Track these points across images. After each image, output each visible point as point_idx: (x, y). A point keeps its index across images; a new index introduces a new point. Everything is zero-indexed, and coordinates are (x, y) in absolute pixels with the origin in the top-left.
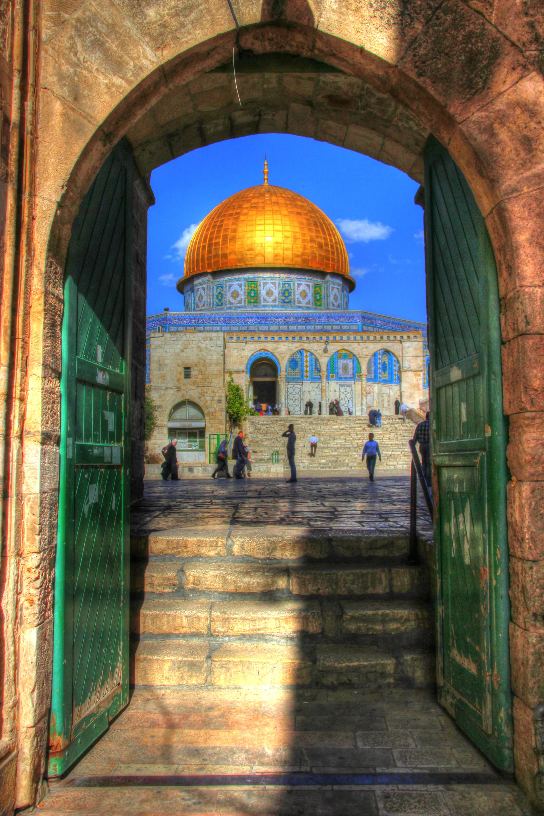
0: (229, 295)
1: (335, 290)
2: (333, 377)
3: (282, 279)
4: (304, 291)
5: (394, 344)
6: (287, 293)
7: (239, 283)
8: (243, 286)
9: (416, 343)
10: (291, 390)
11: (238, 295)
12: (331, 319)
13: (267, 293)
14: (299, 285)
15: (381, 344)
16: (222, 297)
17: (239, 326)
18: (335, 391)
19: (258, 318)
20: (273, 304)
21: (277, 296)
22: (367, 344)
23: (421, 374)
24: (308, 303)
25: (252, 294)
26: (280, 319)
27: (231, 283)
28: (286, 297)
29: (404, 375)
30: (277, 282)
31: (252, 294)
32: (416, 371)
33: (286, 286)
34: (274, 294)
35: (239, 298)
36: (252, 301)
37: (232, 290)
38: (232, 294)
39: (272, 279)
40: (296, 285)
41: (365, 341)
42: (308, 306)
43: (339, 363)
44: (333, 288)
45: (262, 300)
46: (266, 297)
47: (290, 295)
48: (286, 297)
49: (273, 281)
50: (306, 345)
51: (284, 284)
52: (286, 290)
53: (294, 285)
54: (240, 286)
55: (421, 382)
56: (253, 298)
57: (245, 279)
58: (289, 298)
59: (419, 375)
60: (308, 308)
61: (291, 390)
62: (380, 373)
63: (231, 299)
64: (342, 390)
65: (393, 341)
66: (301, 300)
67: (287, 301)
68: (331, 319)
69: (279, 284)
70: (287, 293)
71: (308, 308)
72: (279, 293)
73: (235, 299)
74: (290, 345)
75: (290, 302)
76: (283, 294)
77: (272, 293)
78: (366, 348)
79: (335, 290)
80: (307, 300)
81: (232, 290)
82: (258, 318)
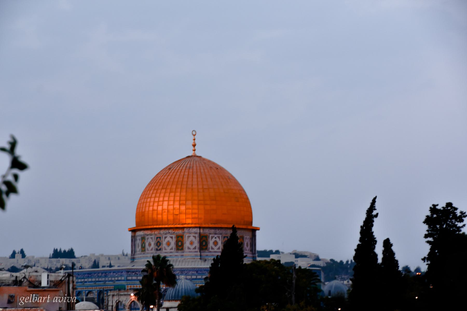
3: (156, 235)
14: (165, 237)
20: (151, 252)
24: (172, 249)
28: (158, 247)
42: (172, 251)
47: (160, 245)
49: (151, 236)
51: (157, 238)
57: (141, 235)
58: (160, 247)
60: (171, 252)
67: (159, 249)
70: (159, 244)
71: (171, 252)
75: (160, 250)
76: (157, 245)
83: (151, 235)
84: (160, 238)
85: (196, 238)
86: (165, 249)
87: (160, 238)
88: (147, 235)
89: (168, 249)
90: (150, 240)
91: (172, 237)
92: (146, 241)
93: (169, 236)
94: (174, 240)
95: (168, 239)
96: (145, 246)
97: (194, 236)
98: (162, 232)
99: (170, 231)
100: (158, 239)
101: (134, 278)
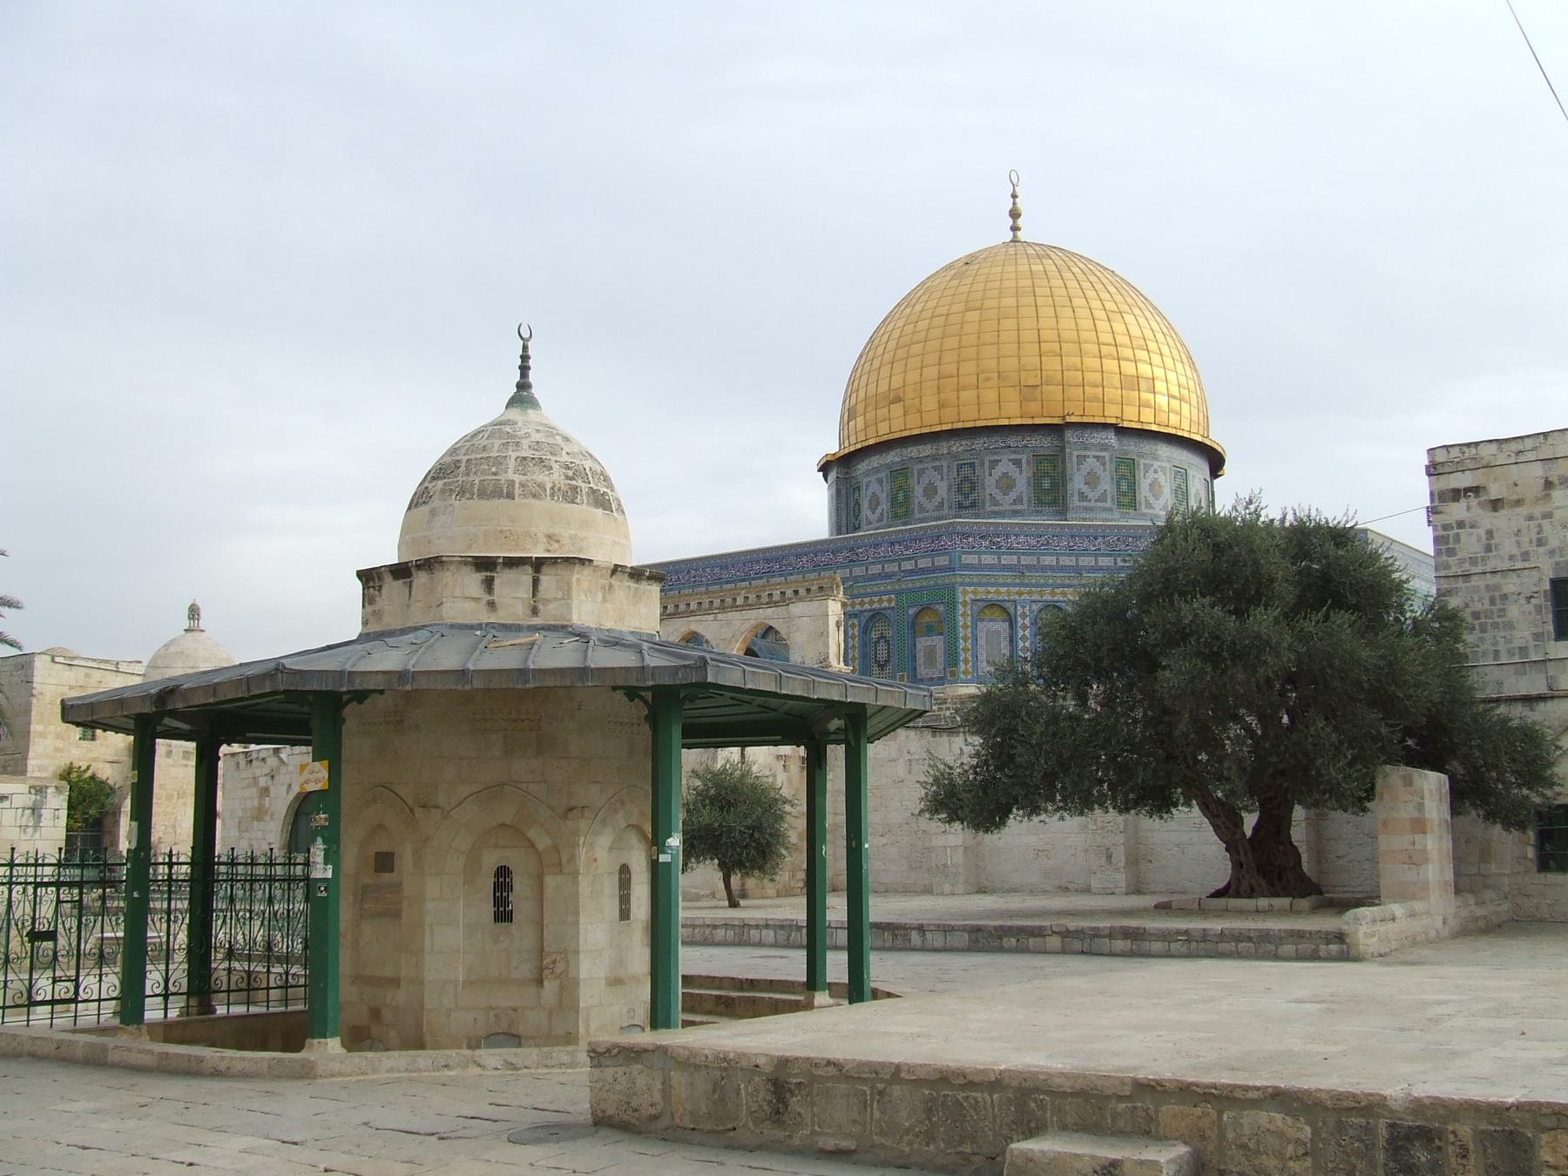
3: (955, 456)
14: (994, 464)
17: (1077, 556)
22: (732, 615)
24: (1018, 500)
25: (901, 497)
28: (966, 496)
30: (945, 464)
31: (901, 497)
33: (966, 471)
39: (935, 458)
44: (1082, 459)
46: (923, 500)
47: (973, 488)
48: (966, 496)
51: (960, 467)
52: (966, 479)
53: (982, 464)
58: (972, 497)
60: (1015, 513)
66: (999, 497)
67: (967, 503)
75: (973, 505)
76: (959, 490)
80: (1013, 495)
82: (767, 561)
83: (935, 458)
84: (972, 465)
86: (995, 502)
87: (972, 465)
88: (920, 460)
89: (1006, 502)
90: (931, 476)
91: (1017, 463)
92: (913, 482)
93: (1005, 457)
96: (907, 498)
98: (979, 443)
99: (1012, 441)
100: (966, 471)
101: (988, 559)
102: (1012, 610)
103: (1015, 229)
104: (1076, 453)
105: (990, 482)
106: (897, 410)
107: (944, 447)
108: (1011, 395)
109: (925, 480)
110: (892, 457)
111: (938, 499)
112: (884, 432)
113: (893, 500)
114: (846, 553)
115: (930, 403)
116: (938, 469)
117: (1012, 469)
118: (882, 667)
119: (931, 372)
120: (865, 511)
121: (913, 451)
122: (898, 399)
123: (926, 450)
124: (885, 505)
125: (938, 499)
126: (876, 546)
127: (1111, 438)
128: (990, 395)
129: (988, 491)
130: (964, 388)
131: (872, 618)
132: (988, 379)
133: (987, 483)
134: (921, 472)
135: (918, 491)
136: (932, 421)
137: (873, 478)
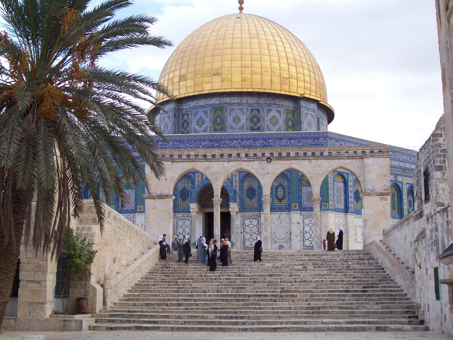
0: (194, 122)
1: (309, 116)
2: (295, 206)
3: (250, 105)
4: (274, 117)
5: (354, 161)
6: (255, 120)
7: (205, 109)
8: (209, 113)
9: (382, 159)
10: (247, 222)
11: (204, 122)
12: (293, 141)
13: (234, 120)
14: (269, 111)
15: (337, 161)
16: (188, 125)
18: (298, 223)
19: (211, 141)
21: (245, 123)
22: (321, 162)
23: (389, 198)
25: (219, 121)
26: (235, 142)
27: (197, 110)
28: (255, 124)
29: (366, 200)
30: (245, 108)
31: (219, 121)
32: (382, 194)
33: (255, 113)
34: (242, 120)
35: (204, 126)
36: (218, 128)
37: (197, 117)
38: (198, 122)
39: (240, 104)
40: (266, 111)
41: (317, 158)
43: (303, 191)
44: (307, 114)
45: (229, 127)
46: (232, 124)
47: (258, 121)
49: (241, 107)
50: (245, 163)
51: (252, 110)
52: (255, 116)
53: (263, 110)
54: (206, 113)
55: (389, 208)
56: (219, 125)
57: (211, 105)
58: (258, 125)
59: (387, 200)
61: (247, 222)
62: (351, 202)
63: (196, 127)
64: (307, 221)
65: (353, 158)
66: (271, 127)
68: (293, 141)
69: (247, 109)
70: (255, 120)
72: (247, 120)
73: (200, 127)
74: (226, 164)
76: (252, 120)
77: (239, 120)
78: (320, 166)
79: (309, 116)
81: (197, 117)
82: (211, 141)
83: (240, 104)
85: (314, 118)
87: (258, 110)
88: (231, 104)
90: (237, 112)
91: (279, 112)
92: (227, 114)
93: (274, 109)
94: (283, 117)
95: (273, 113)
97: (311, 114)
99: (277, 101)
100: (255, 113)
102: (346, 177)
103: (241, 9)
104: (305, 111)
105: (267, 119)
106: (217, 79)
107: (244, 100)
108: (276, 80)
109: (234, 114)
110: (213, 101)
111: (240, 124)
112: (207, 89)
113: (215, 121)
114: (261, 141)
115: (237, 78)
116: (242, 110)
117: (276, 114)
118: (280, 200)
119: (238, 63)
120: (194, 125)
121: (227, 100)
122: (217, 74)
123: (235, 100)
124: (208, 123)
125: (240, 124)
126: (280, 139)
127: (314, 106)
128: (267, 78)
129: (266, 123)
130: (255, 74)
131: (246, 175)
132: (266, 71)
133: (266, 119)
134: (231, 110)
135: (230, 119)
136: (236, 87)
137: (200, 110)
